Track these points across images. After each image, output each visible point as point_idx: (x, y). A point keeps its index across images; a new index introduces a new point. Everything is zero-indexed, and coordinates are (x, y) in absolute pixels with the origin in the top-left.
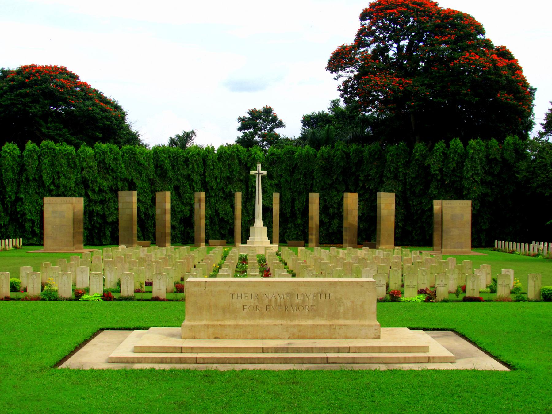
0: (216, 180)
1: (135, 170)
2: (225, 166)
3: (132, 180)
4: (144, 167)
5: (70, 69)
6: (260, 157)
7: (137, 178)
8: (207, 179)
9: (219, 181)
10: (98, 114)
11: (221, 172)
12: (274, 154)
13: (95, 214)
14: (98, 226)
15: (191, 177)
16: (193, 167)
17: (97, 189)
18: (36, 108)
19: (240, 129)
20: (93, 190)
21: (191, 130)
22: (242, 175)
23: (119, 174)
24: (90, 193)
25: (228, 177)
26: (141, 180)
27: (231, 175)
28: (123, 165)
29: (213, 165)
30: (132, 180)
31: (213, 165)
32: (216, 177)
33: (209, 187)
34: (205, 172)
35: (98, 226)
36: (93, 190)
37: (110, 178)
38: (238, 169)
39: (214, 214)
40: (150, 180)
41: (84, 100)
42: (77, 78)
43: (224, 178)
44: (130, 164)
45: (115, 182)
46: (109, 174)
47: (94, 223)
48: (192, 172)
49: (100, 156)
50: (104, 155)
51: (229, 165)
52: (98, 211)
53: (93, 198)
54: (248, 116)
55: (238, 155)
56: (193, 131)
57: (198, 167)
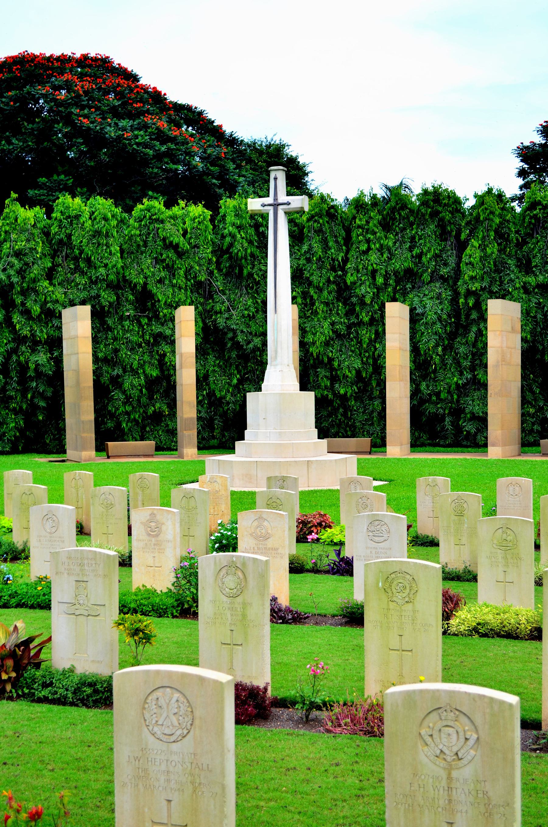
0: (374, 278)
1: (157, 261)
2: (403, 242)
3: (145, 284)
4: (180, 254)
5: (120, 58)
6: (492, 213)
7: (161, 281)
8: (350, 279)
9: (380, 280)
10: (146, 145)
11: (390, 259)
12: (539, 203)
13: (31, 373)
14: (42, 404)
15: (306, 274)
16: (311, 248)
17: (36, 309)
18: (9, 143)
19: (522, 173)
20: (26, 313)
21: (398, 183)
22: (446, 264)
23: (102, 271)
24: (16, 318)
25: (409, 272)
26: (173, 286)
27: (416, 264)
28: (115, 249)
29: (368, 241)
30: (145, 284)
31: (368, 241)
32: (374, 273)
33: (354, 300)
34: (346, 260)
35: (42, 404)
36: (26, 313)
37: (82, 280)
38: (435, 249)
39: (371, 370)
40: (199, 285)
41: (120, 117)
42: (134, 78)
43: (396, 273)
44: (145, 245)
45: (93, 293)
46: (83, 273)
47: (33, 397)
48: (309, 260)
49: (60, 227)
50: (71, 224)
51: (413, 238)
52: (37, 365)
53: (26, 332)
54: (539, 139)
55: (438, 213)
56: (401, 183)
57: (326, 248)
